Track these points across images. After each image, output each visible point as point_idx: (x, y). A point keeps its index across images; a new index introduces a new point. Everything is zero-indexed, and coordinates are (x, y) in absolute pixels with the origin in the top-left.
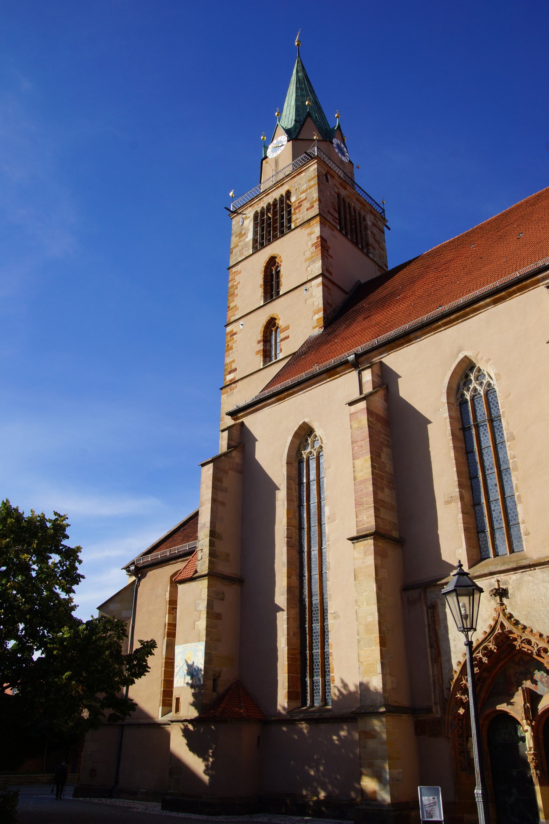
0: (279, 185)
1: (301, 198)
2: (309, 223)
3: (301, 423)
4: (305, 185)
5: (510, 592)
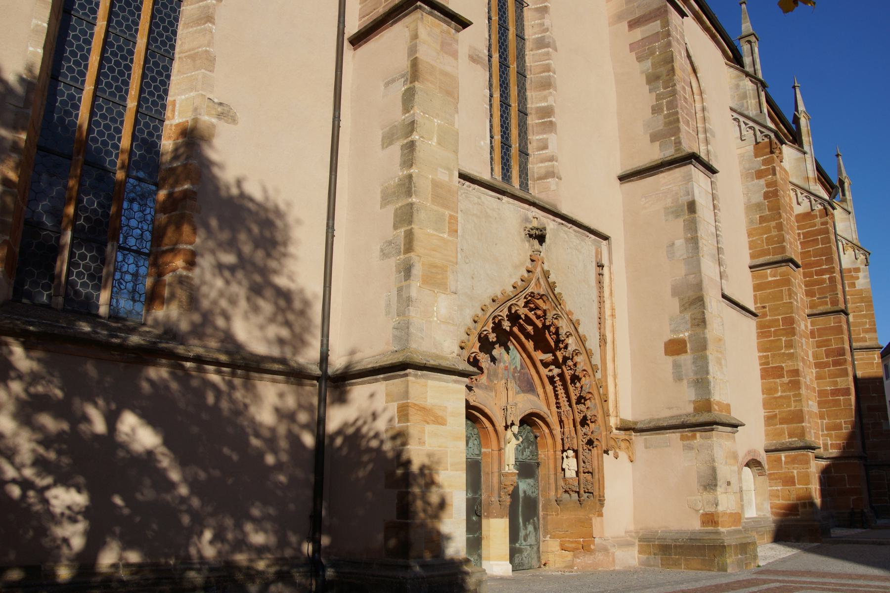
5: (547, 240)
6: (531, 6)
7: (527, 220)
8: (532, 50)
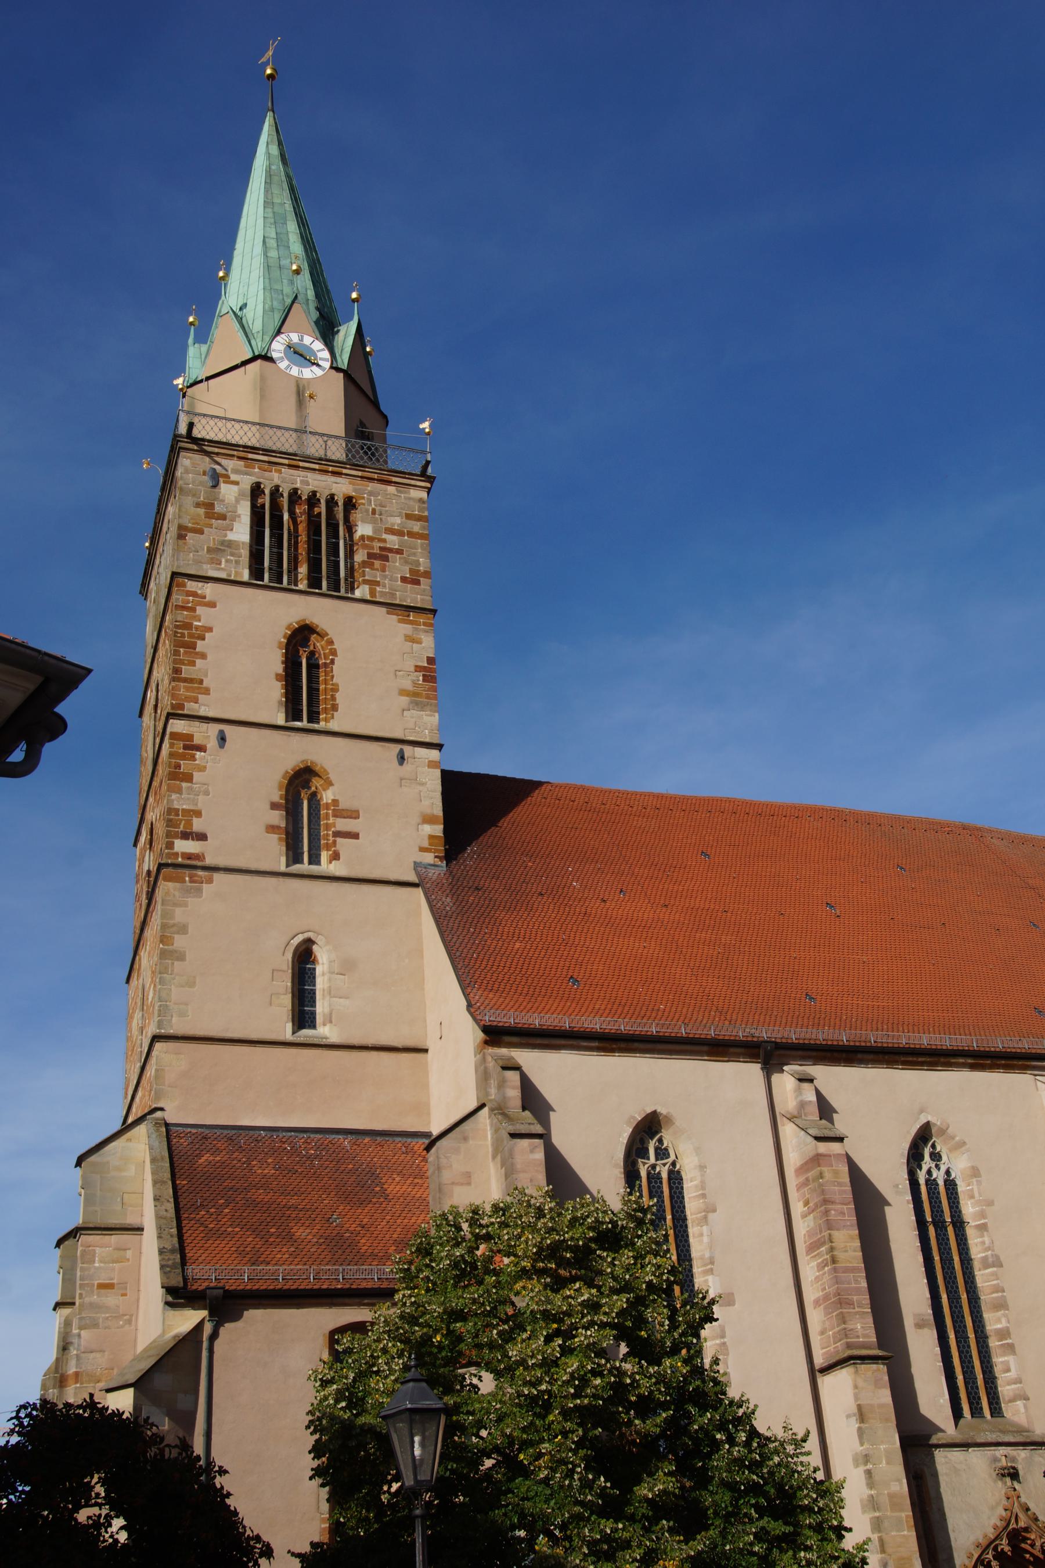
0: (331, 469)
1: (384, 541)
2: (406, 613)
3: (649, 1110)
4: (398, 520)
6: (972, 1224)
7: (996, 1460)
8: (980, 1270)
